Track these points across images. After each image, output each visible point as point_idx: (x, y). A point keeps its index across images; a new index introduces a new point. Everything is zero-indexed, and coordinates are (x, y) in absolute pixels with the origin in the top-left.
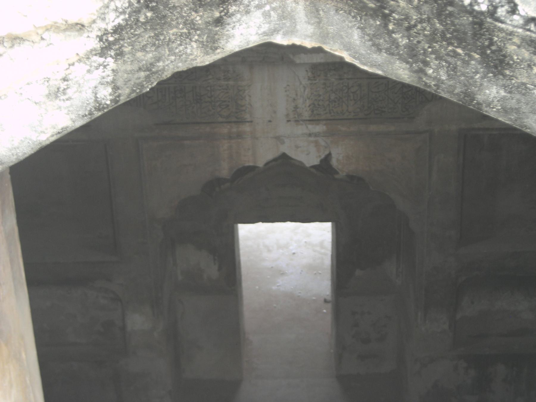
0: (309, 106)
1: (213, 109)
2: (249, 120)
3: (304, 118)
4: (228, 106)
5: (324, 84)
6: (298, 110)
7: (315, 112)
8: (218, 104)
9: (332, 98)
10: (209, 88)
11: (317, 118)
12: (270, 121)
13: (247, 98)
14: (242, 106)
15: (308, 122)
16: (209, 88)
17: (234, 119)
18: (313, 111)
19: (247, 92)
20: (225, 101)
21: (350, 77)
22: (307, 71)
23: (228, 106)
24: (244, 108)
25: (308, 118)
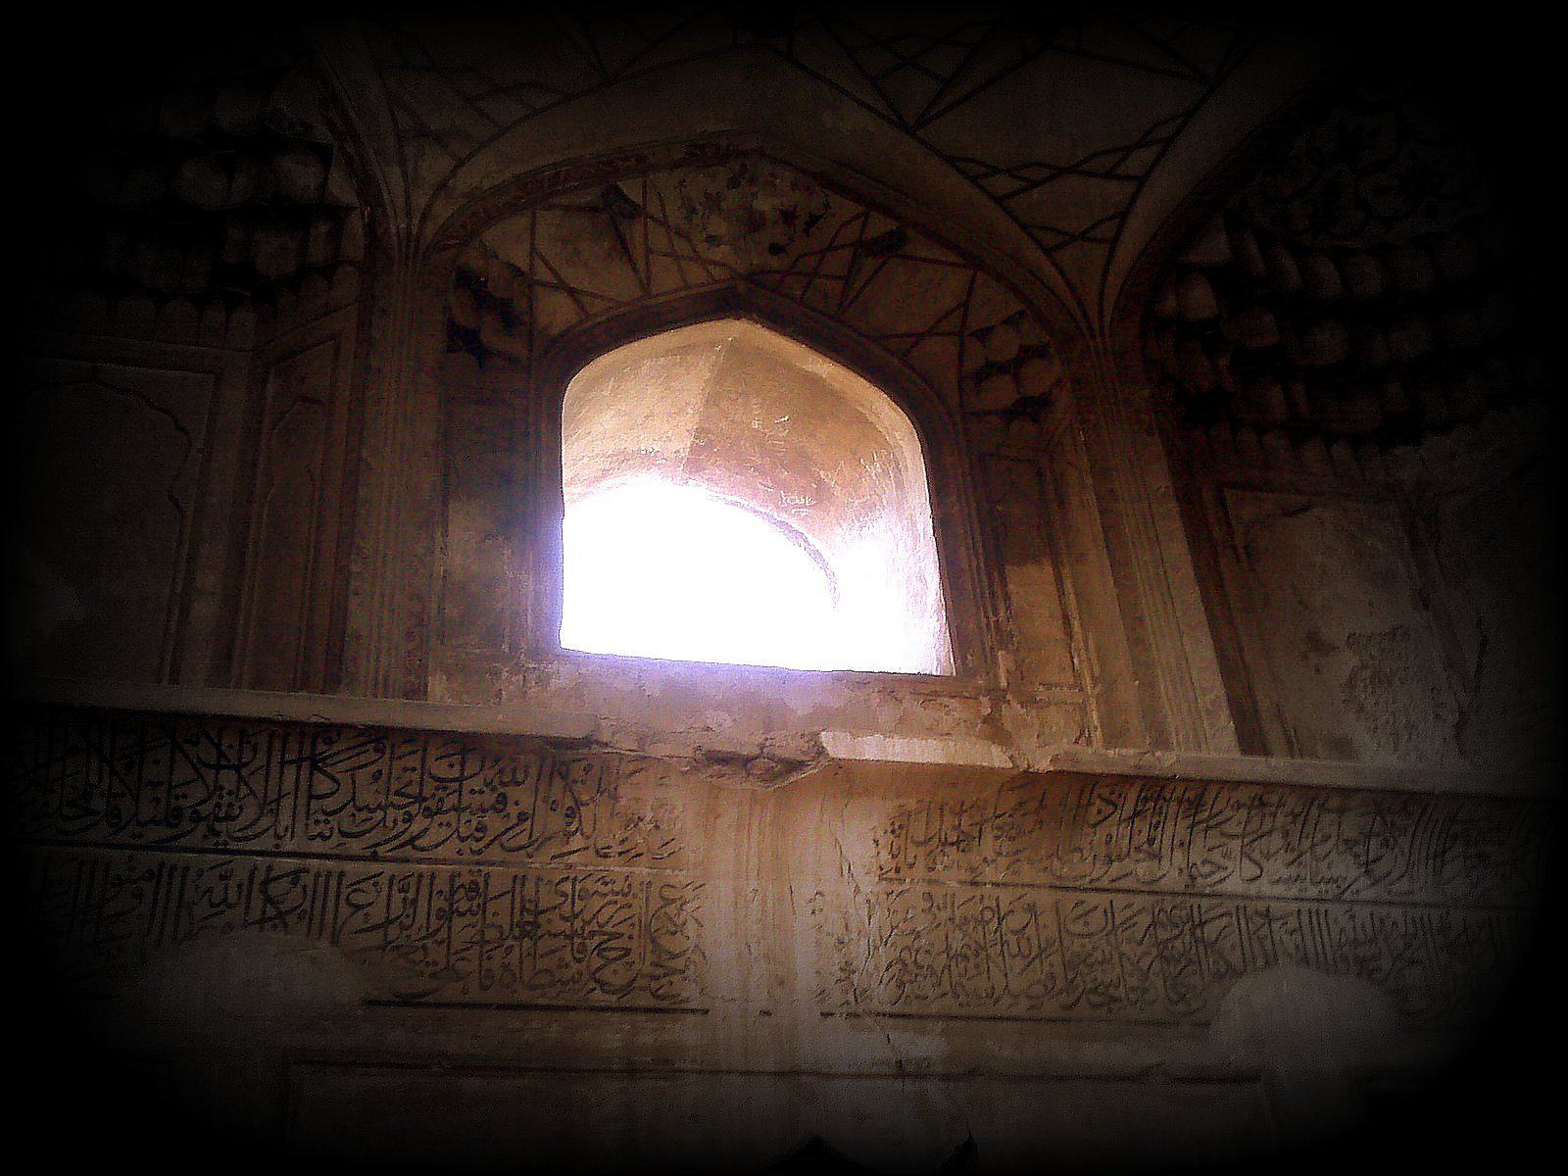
0: (890, 966)
1: (579, 961)
2: (693, 1005)
3: (875, 1006)
4: (628, 952)
5: (929, 896)
6: (855, 977)
7: (908, 988)
8: (597, 939)
9: (956, 945)
10: (567, 887)
11: (914, 1008)
12: (767, 1013)
13: (691, 929)
14: (674, 957)
15: (891, 1022)
16: (567, 887)
17: (645, 1000)
18: (901, 985)
19: (689, 907)
20: (620, 935)
21: (1000, 878)
22: (876, 842)
23: (628, 952)
24: (680, 963)
25: (888, 1009)
